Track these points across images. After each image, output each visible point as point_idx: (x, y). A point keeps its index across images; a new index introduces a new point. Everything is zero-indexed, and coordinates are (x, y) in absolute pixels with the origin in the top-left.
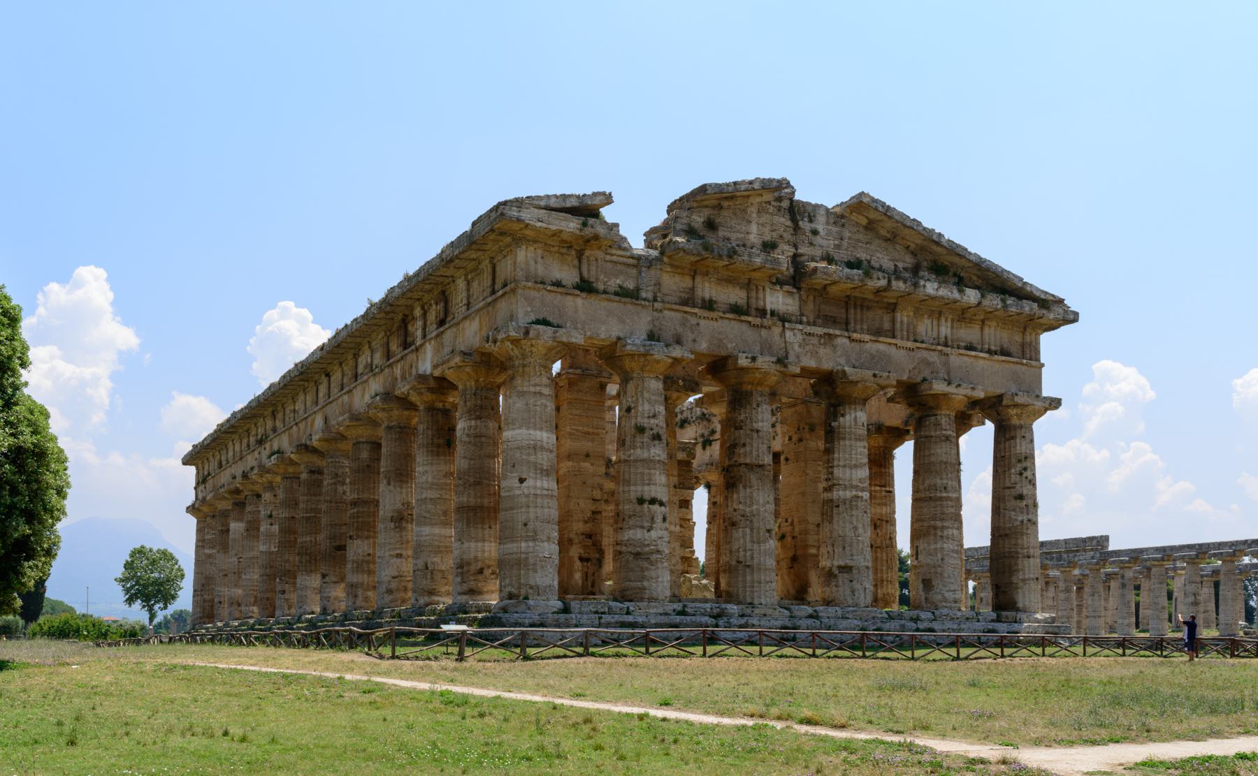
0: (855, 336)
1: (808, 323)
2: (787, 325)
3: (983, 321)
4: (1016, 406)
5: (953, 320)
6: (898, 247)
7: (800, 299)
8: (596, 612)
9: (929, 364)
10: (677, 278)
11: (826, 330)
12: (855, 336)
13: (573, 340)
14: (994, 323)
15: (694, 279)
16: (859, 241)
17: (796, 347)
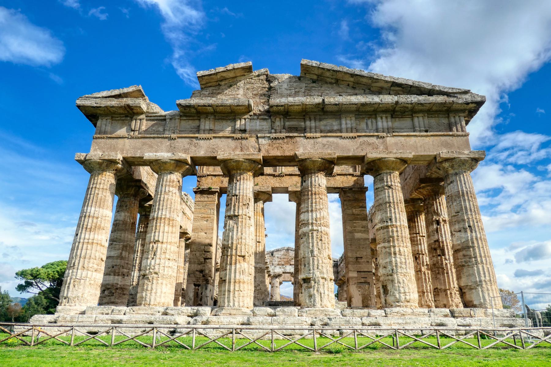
0: (308, 135)
1: (275, 133)
2: (259, 135)
3: (412, 115)
4: (447, 160)
5: (386, 117)
6: (341, 86)
7: (272, 121)
8: (103, 314)
9: (369, 144)
10: (190, 122)
11: (288, 134)
12: (308, 135)
13: (111, 158)
14: (421, 115)
15: (200, 120)
16: (312, 87)
17: (266, 147)
